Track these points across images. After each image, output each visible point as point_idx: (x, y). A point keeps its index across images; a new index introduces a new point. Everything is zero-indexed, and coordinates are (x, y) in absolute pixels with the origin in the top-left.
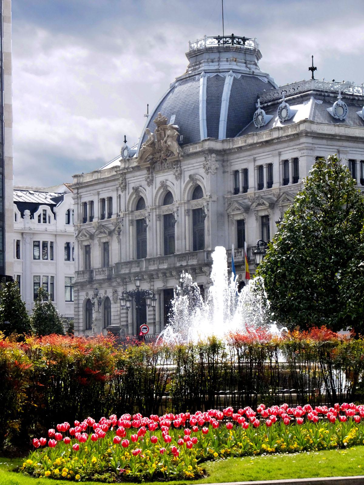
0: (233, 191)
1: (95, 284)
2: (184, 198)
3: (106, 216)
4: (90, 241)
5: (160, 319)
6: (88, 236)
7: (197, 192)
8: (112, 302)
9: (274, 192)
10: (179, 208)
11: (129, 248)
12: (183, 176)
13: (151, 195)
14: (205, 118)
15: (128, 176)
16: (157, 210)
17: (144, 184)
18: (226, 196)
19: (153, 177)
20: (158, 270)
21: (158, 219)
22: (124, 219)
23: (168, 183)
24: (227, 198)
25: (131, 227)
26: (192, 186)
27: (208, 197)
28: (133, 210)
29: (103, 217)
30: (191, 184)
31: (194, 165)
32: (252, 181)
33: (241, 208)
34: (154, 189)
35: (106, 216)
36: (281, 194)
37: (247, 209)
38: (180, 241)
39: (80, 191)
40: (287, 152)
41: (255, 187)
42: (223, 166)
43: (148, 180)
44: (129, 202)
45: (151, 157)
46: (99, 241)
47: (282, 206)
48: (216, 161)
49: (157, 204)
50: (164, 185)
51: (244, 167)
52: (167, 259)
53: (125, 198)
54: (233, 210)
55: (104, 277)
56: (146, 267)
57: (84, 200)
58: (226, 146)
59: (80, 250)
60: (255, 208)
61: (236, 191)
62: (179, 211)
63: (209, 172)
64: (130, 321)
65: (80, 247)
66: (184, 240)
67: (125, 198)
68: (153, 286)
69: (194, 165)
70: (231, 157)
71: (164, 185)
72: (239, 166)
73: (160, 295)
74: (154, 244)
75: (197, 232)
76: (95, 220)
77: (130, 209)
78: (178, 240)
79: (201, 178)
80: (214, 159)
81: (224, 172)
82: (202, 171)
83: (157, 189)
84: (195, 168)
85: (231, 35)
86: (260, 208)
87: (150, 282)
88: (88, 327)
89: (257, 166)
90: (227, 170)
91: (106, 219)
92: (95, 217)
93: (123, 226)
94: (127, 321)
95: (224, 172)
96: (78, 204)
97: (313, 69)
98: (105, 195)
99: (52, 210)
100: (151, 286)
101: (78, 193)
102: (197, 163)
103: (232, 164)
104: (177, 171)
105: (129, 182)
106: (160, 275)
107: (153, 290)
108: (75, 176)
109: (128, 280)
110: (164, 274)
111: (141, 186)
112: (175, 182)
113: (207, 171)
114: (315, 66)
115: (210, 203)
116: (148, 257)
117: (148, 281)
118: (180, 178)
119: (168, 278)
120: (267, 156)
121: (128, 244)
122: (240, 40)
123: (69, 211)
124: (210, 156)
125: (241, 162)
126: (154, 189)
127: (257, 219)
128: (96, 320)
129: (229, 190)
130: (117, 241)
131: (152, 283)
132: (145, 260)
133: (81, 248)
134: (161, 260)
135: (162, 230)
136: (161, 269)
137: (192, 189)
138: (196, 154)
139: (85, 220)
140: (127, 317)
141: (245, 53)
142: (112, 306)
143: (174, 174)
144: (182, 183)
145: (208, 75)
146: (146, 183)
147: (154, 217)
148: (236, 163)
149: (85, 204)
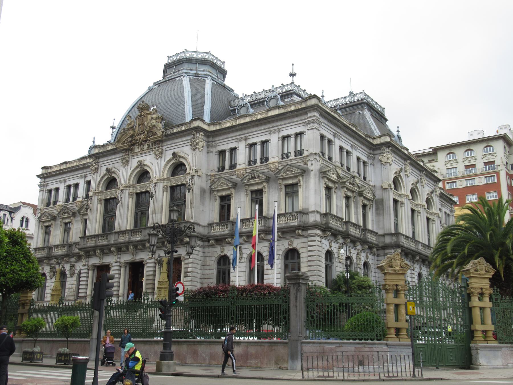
0: (217, 170)
3: (71, 199)
5: (396, 215)
8: (68, 276)
13: (125, 175)
18: (209, 174)
20: (129, 243)
24: (210, 175)
25: (99, 205)
26: (174, 163)
27: (194, 171)
29: (67, 200)
31: (178, 144)
35: (71, 199)
36: (280, 168)
39: (46, 180)
42: (208, 146)
43: (124, 161)
44: (99, 183)
45: (130, 139)
50: (140, 164)
52: (141, 232)
56: (115, 240)
57: (49, 188)
58: (212, 128)
59: (40, 229)
60: (247, 182)
61: (221, 169)
63: (196, 148)
66: (160, 214)
67: (96, 179)
69: (178, 144)
71: (140, 164)
72: (226, 146)
74: (124, 219)
77: (100, 189)
78: (154, 213)
81: (208, 152)
86: (253, 181)
88: (39, 299)
89: (247, 145)
90: (212, 150)
91: (70, 202)
92: (59, 200)
95: (208, 152)
96: (43, 191)
97: (293, 75)
98: (72, 182)
99: (10, 215)
101: (44, 182)
114: (295, 71)
119: (137, 251)
123: (23, 218)
124: (198, 134)
127: (247, 194)
134: (133, 232)
136: (132, 242)
137: (171, 169)
139: (48, 204)
142: (68, 280)
143: (155, 154)
147: (127, 194)
148: (220, 144)
149: (50, 191)
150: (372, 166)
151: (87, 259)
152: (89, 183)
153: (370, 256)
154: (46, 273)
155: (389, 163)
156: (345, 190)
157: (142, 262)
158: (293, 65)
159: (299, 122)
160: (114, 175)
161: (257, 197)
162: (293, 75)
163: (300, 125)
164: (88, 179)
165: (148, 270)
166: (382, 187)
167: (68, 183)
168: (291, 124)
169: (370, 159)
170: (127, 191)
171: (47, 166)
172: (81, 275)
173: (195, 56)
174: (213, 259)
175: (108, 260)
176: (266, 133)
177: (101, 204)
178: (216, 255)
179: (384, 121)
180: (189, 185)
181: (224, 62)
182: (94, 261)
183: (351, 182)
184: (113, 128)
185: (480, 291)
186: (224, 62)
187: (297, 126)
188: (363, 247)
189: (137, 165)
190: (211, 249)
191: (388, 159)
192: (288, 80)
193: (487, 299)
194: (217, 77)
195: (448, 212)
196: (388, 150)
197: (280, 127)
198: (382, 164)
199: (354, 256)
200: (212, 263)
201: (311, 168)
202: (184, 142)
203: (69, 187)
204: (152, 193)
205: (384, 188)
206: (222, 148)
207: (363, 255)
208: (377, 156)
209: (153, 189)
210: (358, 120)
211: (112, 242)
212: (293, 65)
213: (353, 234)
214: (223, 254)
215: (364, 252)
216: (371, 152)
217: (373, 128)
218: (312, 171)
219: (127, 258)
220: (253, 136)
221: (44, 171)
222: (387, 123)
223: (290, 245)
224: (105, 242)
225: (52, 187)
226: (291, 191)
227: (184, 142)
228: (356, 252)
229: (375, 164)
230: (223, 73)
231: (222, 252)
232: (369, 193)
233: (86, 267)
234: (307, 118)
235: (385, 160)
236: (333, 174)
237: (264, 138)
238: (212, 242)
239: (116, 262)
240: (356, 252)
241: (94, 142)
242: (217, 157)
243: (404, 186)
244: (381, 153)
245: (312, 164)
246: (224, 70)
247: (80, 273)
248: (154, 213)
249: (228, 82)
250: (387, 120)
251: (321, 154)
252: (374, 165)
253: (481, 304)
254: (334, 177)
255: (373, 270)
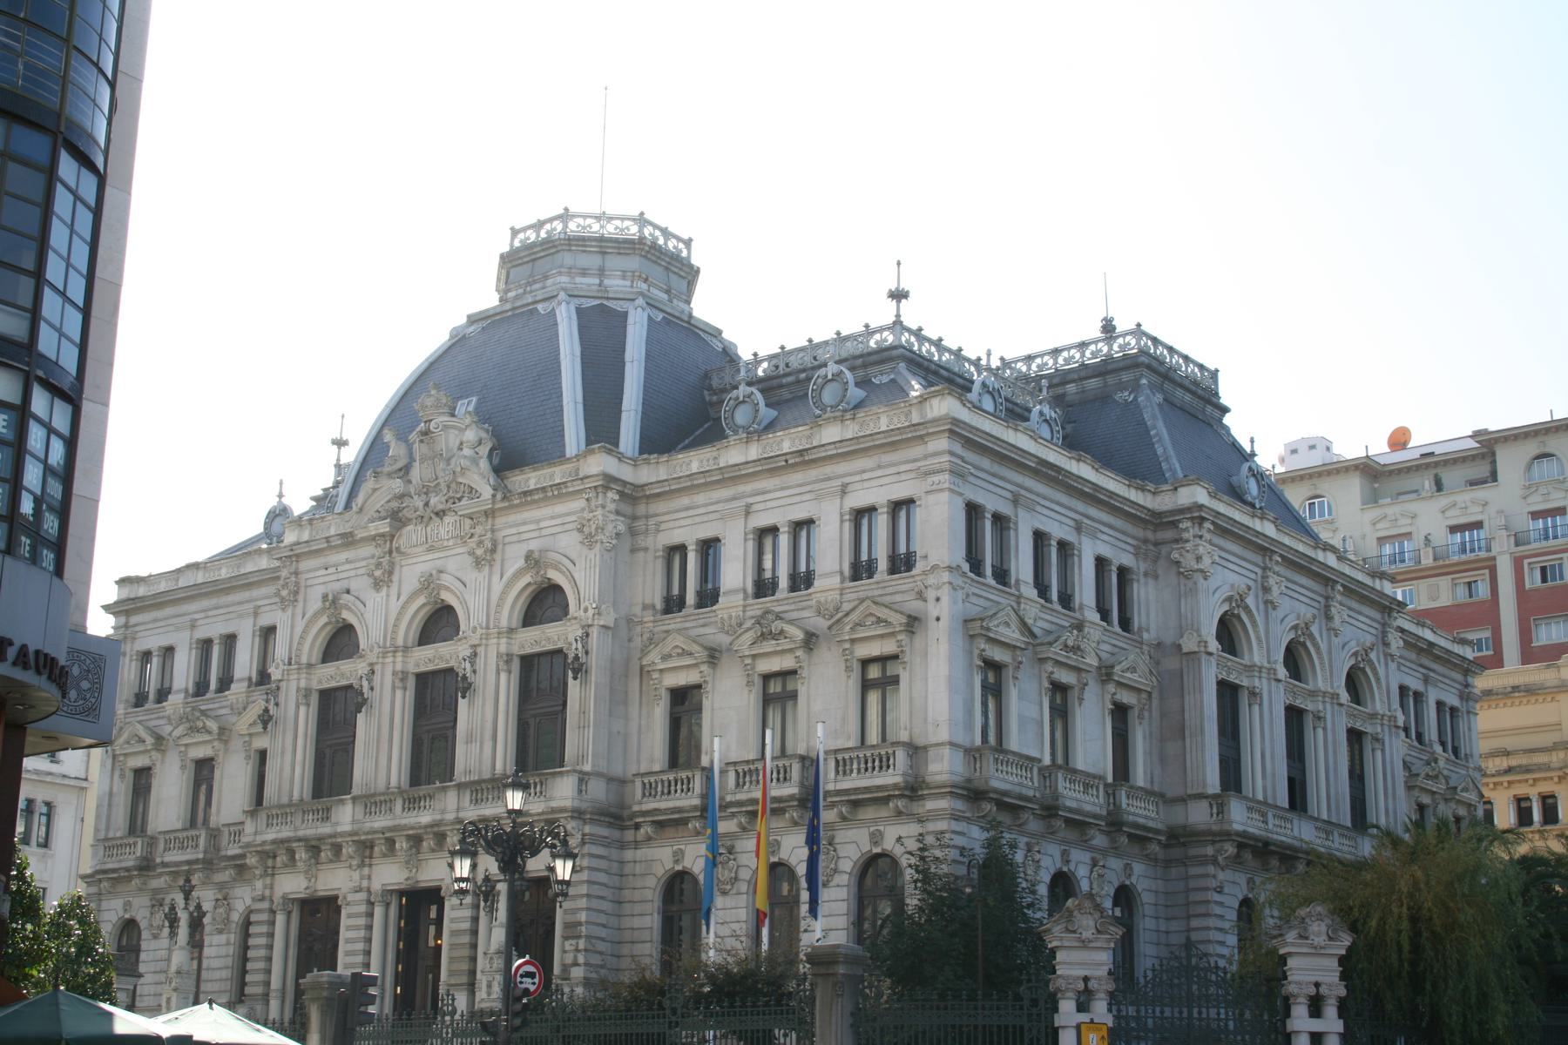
0: (659, 605)
1: (161, 875)
2: (497, 620)
3: (213, 685)
4: (155, 755)
6: (150, 740)
7: (545, 602)
9: (822, 597)
10: (481, 650)
11: (293, 769)
12: (498, 556)
13: (382, 616)
14: (580, 398)
15: (305, 565)
16: (399, 658)
17: (361, 585)
19: (392, 564)
21: (398, 684)
22: (283, 684)
23: (446, 580)
27: (591, 612)
28: (313, 661)
29: (201, 688)
30: (527, 579)
31: (542, 525)
32: (734, 573)
33: (696, 648)
34: (393, 598)
35: (213, 685)
36: (846, 607)
37: (714, 656)
38: (475, 748)
39: (134, 619)
40: (874, 483)
41: (745, 591)
43: (378, 573)
46: (183, 755)
47: (853, 641)
48: (618, 513)
49: (400, 642)
51: (706, 532)
53: (292, 627)
54: (665, 658)
55: (193, 857)
56: (353, 822)
61: (673, 604)
62: (480, 662)
64: (275, 983)
65: (117, 773)
66: (488, 745)
67: (292, 627)
68: (369, 878)
70: (660, 507)
72: (688, 533)
73: (388, 905)
75: (531, 721)
76: (175, 699)
78: (470, 739)
79: (567, 563)
80: (612, 507)
82: (569, 542)
83: (403, 598)
84: (544, 532)
85: (636, 213)
86: (769, 646)
87: (361, 865)
91: (208, 696)
93: (277, 704)
94: (268, 984)
95: (633, 551)
97: (898, 295)
98: (214, 629)
100: (362, 878)
102: (552, 518)
103: (663, 526)
104: (480, 543)
105: (309, 582)
106: (402, 844)
107: (369, 891)
108: (123, 582)
109: (282, 859)
110: (416, 841)
111: (348, 592)
112: (471, 576)
113: (589, 540)
114: (904, 286)
115: (594, 632)
116: (356, 791)
117: (354, 862)
118: (491, 563)
120: (797, 499)
121: (288, 758)
122: (657, 233)
125: (698, 519)
126: (393, 598)
128: (178, 972)
129: (648, 601)
130: (243, 755)
131: (366, 871)
132: (354, 799)
133: (122, 776)
135: (409, 717)
138: (556, 493)
140: (268, 972)
141: (667, 269)
144: (496, 578)
145: (577, 301)
146: (369, 581)
147: (388, 679)
148: (671, 525)
150: (1151, 582)
151: (268, 880)
152: (268, 632)
153: (1138, 868)
154: (138, 918)
155: (1202, 571)
156: (1049, 667)
157: (438, 889)
158: (899, 264)
159: (903, 468)
160: (346, 615)
161: (777, 693)
162: (898, 295)
163: (904, 477)
164: (265, 621)
165: (455, 914)
166: (1179, 647)
167: (201, 634)
168: (879, 473)
169: (1145, 560)
170: (389, 670)
171: (133, 574)
172: (252, 930)
173: (596, 227)
174: (651, 882)
175: (336, 880)
176: (805, 497)
177: (308, 705)
178: (660, 871)
179: (1217, 413)
180: (577, 658)
181: (690, 240)
182: (292, 884)
183: (1070, 643)
184: (340, 443)
185: (1313, 991)
186: (690, 240)
187: (896, 478)
188: (1113, 841)
189: (417, 585)
190: (642, 853)
191: (1199, 559)
192: (884, 314)
193: (1331, 1011)
194: (668, 292)
195: (1452, 700)
196: (1196, 530)
197: (847, 480)
198: (1180, 573)
199: (1082, 872)
200: (649, 894)
201: (933, 610)
202: (559, 521)
203: (206, 644)
204: (465, 678)
205: (1185, 650)
206: (676, 538)
207: (1115, 863)
208: (1164, 550)
209: (468, 665)
210: (1133, 414)
211: (347, 828)
212: (899, 264)
213: (1068, 803)
214: (679, 868)
215: (1118, 856)
216: (1150, 535)
217: (1160, 451)
218: (938, 619)
219: (390, 874)
220: (769, 505)
221: (127, 592)
222: (1227, 420)
223: (876, 843)
224: (325, 829)
225: (153, 642)
226: (878, 677)
227: (559, 521)
228: (1086, 857)
229: (1160, 572)
230: (690, 274)
231: (676, 862)
232: (1133, 670)
233: (266, 905)
234: (926, 457)
235: (1189, 562)
236: (1007, 624)
237: (800, 514)
238: (646, 830)
239: (358, 890)
240: (1086, 857)
241: (281, 496)
242: (660, 565)
243: (1259, 639)
244: (1177, 541)
245: (938, 599)
246: (691, 266)
247: (247, 923)
248: (470, 739)
249: (705, 306)
250: (1225, 410)
251: (966, 567)
252: (1156, 577)
253: (1316, 1025)
254: (1012, 634)
255: (1148, 910)
